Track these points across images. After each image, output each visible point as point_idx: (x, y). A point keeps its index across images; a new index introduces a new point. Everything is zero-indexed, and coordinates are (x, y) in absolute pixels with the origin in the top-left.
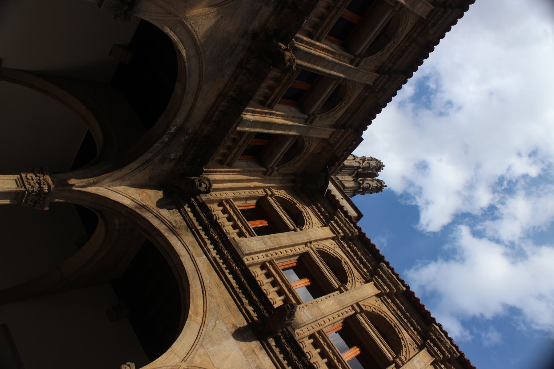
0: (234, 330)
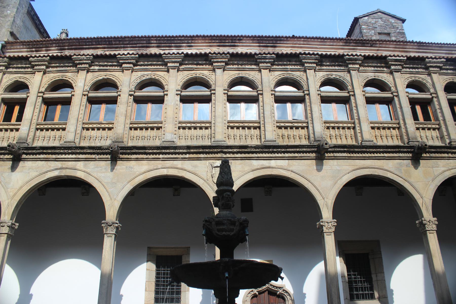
0: (10, 170)
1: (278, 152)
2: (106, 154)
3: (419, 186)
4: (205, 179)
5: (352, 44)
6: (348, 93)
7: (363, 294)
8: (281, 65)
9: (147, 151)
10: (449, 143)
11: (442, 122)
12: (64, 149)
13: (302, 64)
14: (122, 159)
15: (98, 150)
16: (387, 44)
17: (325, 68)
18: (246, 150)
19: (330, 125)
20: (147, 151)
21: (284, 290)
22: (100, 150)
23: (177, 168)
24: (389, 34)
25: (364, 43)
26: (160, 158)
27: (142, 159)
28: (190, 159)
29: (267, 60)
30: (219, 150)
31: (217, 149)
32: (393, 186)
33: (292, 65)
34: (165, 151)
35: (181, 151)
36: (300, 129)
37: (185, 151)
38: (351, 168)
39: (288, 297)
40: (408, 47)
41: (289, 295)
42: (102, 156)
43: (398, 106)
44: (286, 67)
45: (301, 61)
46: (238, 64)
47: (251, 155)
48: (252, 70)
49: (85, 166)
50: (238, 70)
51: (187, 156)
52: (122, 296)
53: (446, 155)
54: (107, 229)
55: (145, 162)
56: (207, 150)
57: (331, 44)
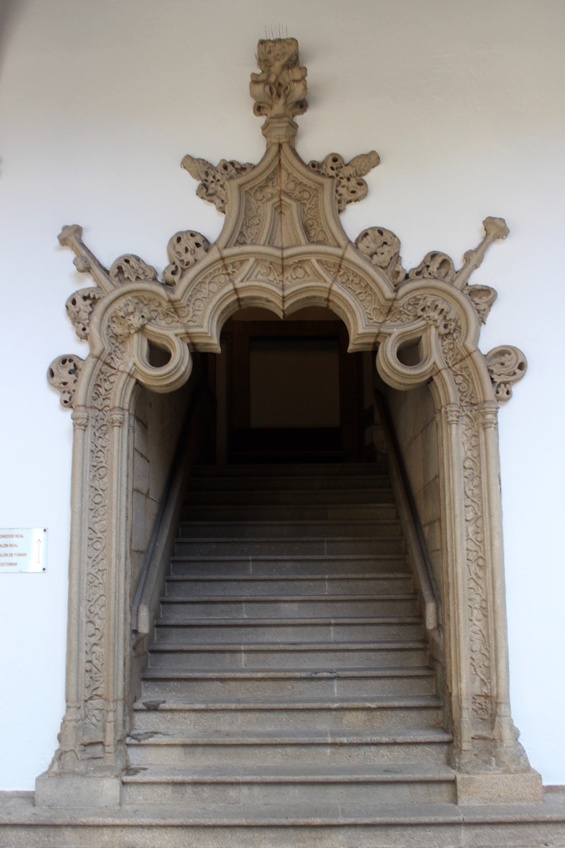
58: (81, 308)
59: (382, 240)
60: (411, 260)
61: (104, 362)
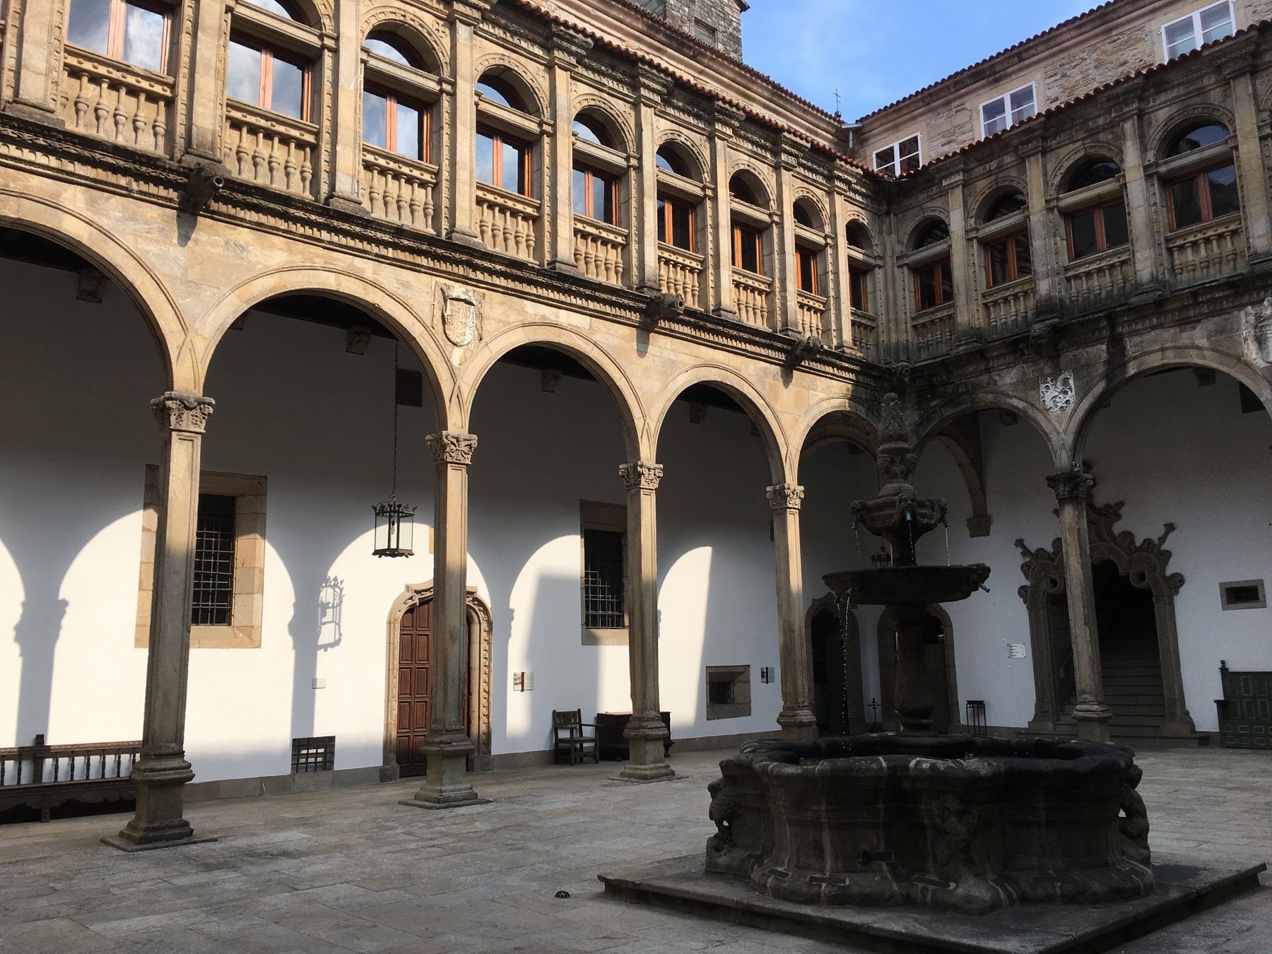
1: (577, 295)
2: (167, 184)
3: (786, 420)
4: (428, 323)
5: (660, 37)
6: (440, 82)
7: (603, 616)
8: (594, 71)
9: (292, 211)
10: (836, 348)
11: (832, 301)
12: (19, 129)
13: (635, 87)
14: (214, 215)
15: (142, 164)
16: (722, 65)
17: (670, 110)
18: (519, 273)
19: (240, 119)
20: (292, 211)
21: (476, 599)
22: (149, 166)
23: (362, 279)
24: (712, 31)
25: (683, 44)
26: (322, 241)
27: (274, 231)
28: (395, 263)
29: (574, 48)
30: (464, 258)
31: (462, 253)
32: (742, 411)
33: (614, 79)
34: (346, 226)
35: (379, 235)
36: (143, 97)
37: (387, 238)
38: (692, 362)
39: (481, 615)
40: (755, 88)
41: (486, 610)
42: (152, 189)
43: (547, 160)
44: (605, 81)
45: (635, 77)
46: (505, 29)
47: (526, 288)
48: (533, 57)
49: (91, 203)
50: (503, 44)
51: (390, 252)
52: (65, 603)
53: (829, 369)
54: (180, 416)
55: (278, 241)
56: (439, 251)
57: (621, 17)
58: (1025, 569)
59: (1128, 535)
60: (1138, 542)
61: (1035, 587)
